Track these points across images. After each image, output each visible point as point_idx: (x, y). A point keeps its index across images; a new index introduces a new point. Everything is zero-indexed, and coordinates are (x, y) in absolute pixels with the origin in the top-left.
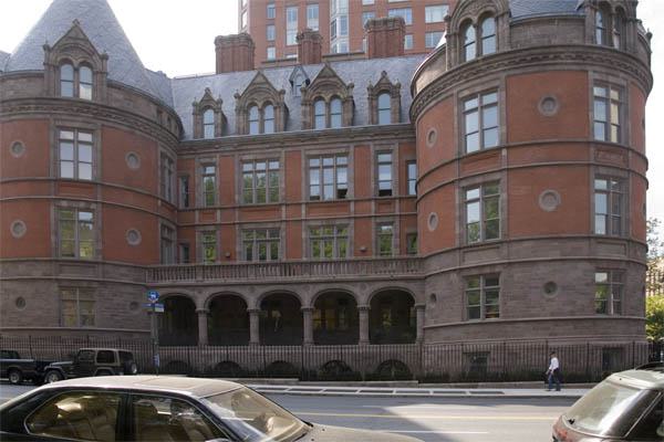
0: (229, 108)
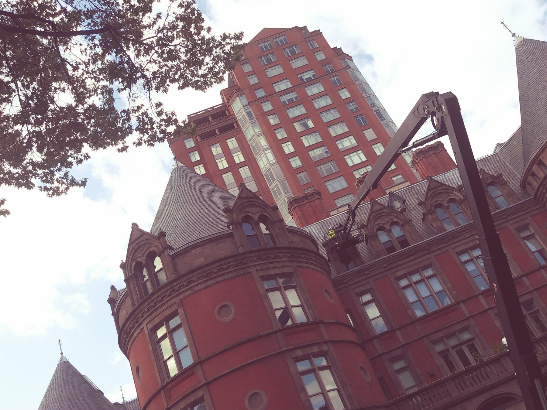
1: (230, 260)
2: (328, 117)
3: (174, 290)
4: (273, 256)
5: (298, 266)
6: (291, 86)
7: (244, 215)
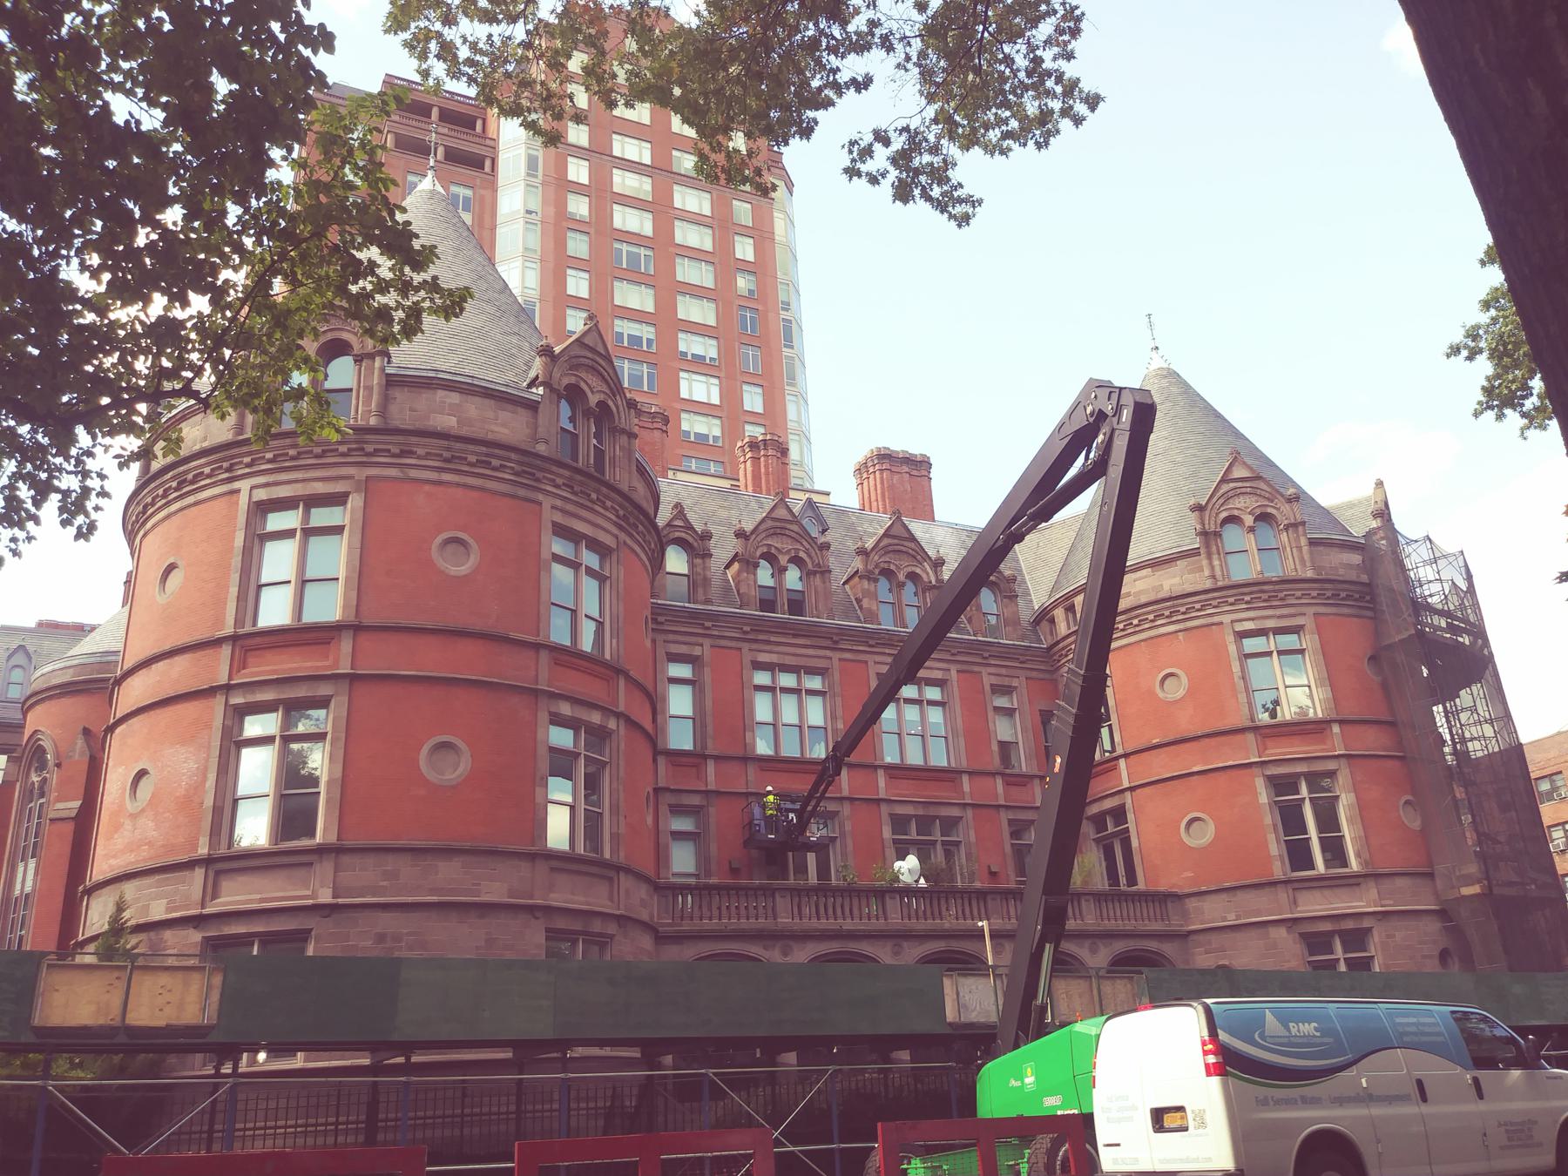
0: (723, 549)
1: (513, 456)
2: (689, 272)
3: (363, 449)
4: (594, 496)
5: (625, 542)
6: (649, 163)
7: (573, 380)
